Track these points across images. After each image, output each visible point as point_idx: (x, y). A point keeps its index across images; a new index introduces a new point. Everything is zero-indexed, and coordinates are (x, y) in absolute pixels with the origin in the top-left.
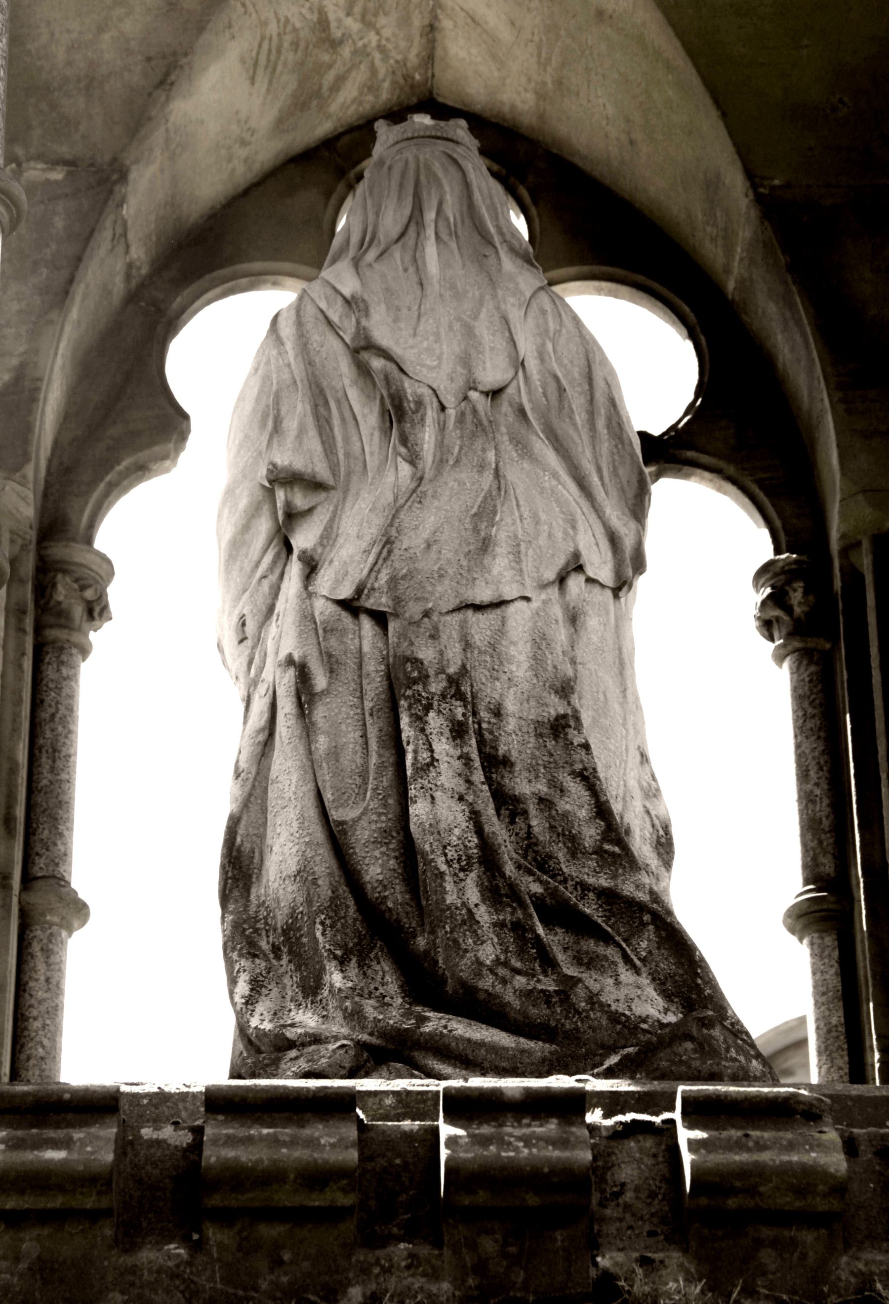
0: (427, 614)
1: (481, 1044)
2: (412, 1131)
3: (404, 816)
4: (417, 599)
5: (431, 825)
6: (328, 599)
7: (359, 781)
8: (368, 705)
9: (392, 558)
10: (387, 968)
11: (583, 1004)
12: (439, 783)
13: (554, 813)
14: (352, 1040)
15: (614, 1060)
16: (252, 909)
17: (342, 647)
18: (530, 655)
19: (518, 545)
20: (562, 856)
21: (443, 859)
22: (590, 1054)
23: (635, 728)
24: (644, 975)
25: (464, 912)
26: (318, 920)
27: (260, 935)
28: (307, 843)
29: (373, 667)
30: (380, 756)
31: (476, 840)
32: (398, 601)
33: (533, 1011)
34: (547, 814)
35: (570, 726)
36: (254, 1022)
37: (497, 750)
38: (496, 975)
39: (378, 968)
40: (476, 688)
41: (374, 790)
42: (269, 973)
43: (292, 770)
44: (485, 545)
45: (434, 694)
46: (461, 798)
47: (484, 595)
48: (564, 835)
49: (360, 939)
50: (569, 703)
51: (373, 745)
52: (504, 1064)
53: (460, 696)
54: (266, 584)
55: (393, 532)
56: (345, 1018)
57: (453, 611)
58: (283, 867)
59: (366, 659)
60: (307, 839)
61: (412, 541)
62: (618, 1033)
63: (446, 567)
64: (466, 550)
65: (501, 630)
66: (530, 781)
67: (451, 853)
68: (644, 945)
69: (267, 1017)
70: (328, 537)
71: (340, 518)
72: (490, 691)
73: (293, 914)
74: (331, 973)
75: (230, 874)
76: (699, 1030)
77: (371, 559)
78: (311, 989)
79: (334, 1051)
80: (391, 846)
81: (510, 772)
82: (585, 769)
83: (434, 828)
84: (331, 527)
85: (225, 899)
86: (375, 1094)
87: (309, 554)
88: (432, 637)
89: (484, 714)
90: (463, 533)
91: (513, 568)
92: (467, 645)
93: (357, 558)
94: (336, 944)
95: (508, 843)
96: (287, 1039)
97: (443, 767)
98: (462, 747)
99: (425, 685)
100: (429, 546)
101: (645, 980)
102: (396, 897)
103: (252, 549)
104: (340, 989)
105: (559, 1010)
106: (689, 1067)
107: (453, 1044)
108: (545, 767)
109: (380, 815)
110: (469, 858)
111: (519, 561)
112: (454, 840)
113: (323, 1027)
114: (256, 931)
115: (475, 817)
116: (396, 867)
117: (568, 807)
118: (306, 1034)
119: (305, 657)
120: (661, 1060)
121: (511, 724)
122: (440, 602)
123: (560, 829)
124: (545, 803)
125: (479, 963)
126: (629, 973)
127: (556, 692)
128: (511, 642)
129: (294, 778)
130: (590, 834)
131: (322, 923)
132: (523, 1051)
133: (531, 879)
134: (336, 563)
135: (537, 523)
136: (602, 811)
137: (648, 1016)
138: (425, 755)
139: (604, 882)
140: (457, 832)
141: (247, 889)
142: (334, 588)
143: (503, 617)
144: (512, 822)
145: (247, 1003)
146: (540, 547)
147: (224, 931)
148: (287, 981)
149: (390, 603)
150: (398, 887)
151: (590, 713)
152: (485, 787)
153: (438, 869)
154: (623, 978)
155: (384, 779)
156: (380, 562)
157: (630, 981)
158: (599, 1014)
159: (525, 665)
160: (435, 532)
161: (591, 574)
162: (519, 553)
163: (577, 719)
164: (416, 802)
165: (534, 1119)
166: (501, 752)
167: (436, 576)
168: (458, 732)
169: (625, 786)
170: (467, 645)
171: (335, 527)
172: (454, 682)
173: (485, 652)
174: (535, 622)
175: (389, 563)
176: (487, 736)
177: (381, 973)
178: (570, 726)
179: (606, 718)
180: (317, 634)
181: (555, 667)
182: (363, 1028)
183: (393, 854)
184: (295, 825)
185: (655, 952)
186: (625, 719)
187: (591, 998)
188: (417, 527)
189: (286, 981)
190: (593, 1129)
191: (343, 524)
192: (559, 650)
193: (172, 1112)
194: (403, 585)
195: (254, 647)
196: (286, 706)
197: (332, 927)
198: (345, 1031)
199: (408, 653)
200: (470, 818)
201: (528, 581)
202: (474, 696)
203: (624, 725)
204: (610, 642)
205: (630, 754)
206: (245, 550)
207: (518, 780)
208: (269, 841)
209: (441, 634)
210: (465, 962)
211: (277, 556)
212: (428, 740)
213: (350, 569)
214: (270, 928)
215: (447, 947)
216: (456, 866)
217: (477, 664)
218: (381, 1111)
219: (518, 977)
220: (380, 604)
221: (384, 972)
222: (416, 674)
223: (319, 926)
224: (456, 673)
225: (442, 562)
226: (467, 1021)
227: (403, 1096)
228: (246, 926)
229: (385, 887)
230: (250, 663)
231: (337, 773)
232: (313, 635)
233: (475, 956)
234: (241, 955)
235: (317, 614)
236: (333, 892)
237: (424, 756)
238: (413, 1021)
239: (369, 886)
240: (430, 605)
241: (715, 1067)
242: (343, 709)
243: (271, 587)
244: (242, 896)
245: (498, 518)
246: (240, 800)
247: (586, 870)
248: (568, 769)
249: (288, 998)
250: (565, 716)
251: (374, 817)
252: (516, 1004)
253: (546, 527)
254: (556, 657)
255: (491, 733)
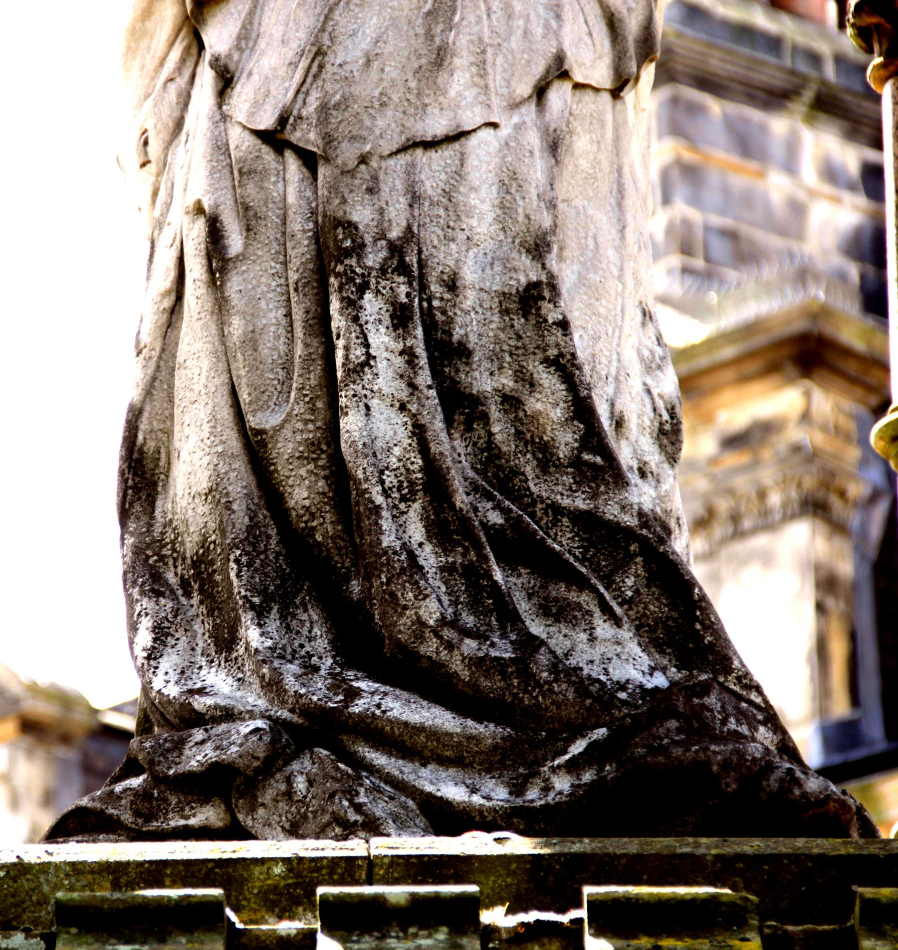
0: (364, 160)
1: (420, 729)
2: (289, 935)
3: (332, 430)
4: (353, 138)
5: (364, 444)
6: (245, 127)
7: (282, 374)
8: (293, 276)
9: (323, 76)
10: (315, 617)
11: (545, 674)
12: (376, 388)
13: (521, 414)
14: (269, 718)
15: (578, 747)
16: (158, 529)
17: (262, 195)
18: (496, 202)
19: (484, 52)
20: (529, 471)
21: (379, 488)
22: (553, 736)
23: (635, 279)
24: (626, 627)
25: (403, 557)
26: (232, 557)
27: (166, 564)
28: (220, 455)
29: (298, 224)
30: (307, 345)
31: (420, 461)
32: (328, 139)
33: (485, 683)
34: (512, 416)
35: (544, 298)
36: (158, 683)
37: (451, 335)
38: (440, 638)
39: (304, 617)
40: (426, 253)
41: (300, 390)
42: (175, 616)
43: (203, 355)
44: (440, 58)
45: (371, 268)
46: (403, 408)
47: (436, 125)
48: (532, 441)
49: (284, 581)
50: (544, 267)
51: (299, 332)
52: (448, 753)
53: (403, 269)
54: (173, 88)
55: (326, 41)
56: (262, 687)
57: (398, 152)
58: (192, 480)
59: (290, 213)
60: (220, 449)
61: (348, 53)
62: (588, 709)
63: (389, 92)
64: (416, 66)
65: (459, 174)
66: (491, 374)
67: (390, 479)
68: (630, 582)
69: (173, 677)
70: (247, 38)
71: (262, 9)
72: (443, 256)
73: (203, 543)
74: (247, 629)
75: (130, 483)
76: (688, 700)
77: (298, 76)
78: (225, 642)
79: (246, 736)
80: (321, 463)
81: (467, 364)
82: (561, 355)
83: (369, 450)
84: (251, 23)
85: (124, 515)
86: (262, 861)
87: (222, 63)
88: (370, 191)
89: (435, 288)
90: (413, 41)
91: (476, 85)
92: (415, 198)
93: (281, 73)
94: (253, 589)
95: (463, 458)
96: (194, 710)
97: (381, 366)
98: (405, 339)
99: (360, 258)
100: (368, 62)
101: (626, 633)
102: (325, 527)
103: (155, 41)
104: (256, 650)
105: (515, 682)
106: (668, 756)
107: (388, 728)
108: (511, 354)
109: (306, 422)
110: (412, 484)
111: (483, 75)
112: (394, 462)
113: (239, 694)
114: (162, 558)
115: (419, 431)
116: (327, 489)
117: (539, 406)
118: (216, 707)
119: (217, 206)
120: (636, 746)
121: (470, 298)
122: (381, 142)
123: (529, 436)
124: (511, 402)
125: (420, 622)
126: (607, 625)
127: (528, 251)
128: (472, 189)
129: (206, 364)
130: (565, 440)
131: (237, 561)
132: (470, 738)
133: (489, 505)
134: (255, 77)
135: (510, 17)
136: (582, 409)
137: (628, 681)
138: (358, 353)
139: (581, 503)
140: (397, 451)
141: (152, 503)
142: (253, 113)
143: (462, 154)
144: (469, 429)
145: (148, 658)
146: (512, 52)
147: (124, 556)
148: (197, 627)
149: (320, 142)
150: (328, 516)
151: (575, 267)
152: (433, 393)
153: (373, 502)
154: (599, 632)
155: (312, 376)
156: (309, 80)
157: (608, 636)
158: (564, 686)
159: (490, 217)
160: (377, 42)
161: (579, 78)
162: (484, 62)
163: (553, 287)
164: (347, 414)
165: (421, 928)
166: (456, 338)
167: (376, 104)
168: (400, 318)
169: (619, 361)
170: (415, 198)
171: (256, 21)
172: (396, 249)
173: (438, 203)
174: (503, 158)
175: (320, 83)
176: (439, 317)
177: (308, 624)
178: (544, 298)
179: (596, 272)
180: (232, 173)
181: (528, 217)
182: (283, 703)
183: (322, 473)
184: (206, 428)
185: (644, 590)
186: (621, 269)
187: (555, 665)
188: (354, 34)
189: (196, 627)
190: (490, 932)
191: (266, 20)
192: (533, 194)
193: (33, 885)
194: (336, 117)
195: (159, 174)
196: (196, 269)
197: (249, 565)
198: (262, 703)
199: (340, 214)
200: (414, 434)
201: (495, 101)
202: (422, 264)
203: (620, 278)
204: (605, 165)
205: (627, 317)
206: (144, 44)
207: (477, 373)
208: (177, 444)
209: (382, 186)
210: (405, 621)
211: (187, 51)
212: (362, 332)
213: (272, 88)
214: (178, 557)
215: (382, 601)
216: (396, 495)
217: (428, 220)
218: (269, 882)
219: (467, 641)
220: (308, 141)
221: (312, 623)
222: (348, 243)
223: (233, 565)
224: (399, 238)
225: (384, 84)
226: (405, 695)
227: (295, 864)
228: (149, 553)
229: (312, 515)
230: (155, 194)
231: (254, 367)
232: (228, 174)
233: (416, 613)
234: (143, 593)
235: (232, 147)
236: (251, 519)
237: (358, 353)
238: (341, 697)
239: (294, 513)
240: (368, 148)
241: (702, 755)
242: (263, 280)
243: (179, 95)
244: (144, 512)
245: (457, 18)
246: (141, 385)
247: (560, 488)
248: (540, 356)
249: (199, 650)
250: (537, 285)
251: (299, 425)
252: (465, 675)
253: (521, 22)
254: (530, 203)
255: (444, 313)
